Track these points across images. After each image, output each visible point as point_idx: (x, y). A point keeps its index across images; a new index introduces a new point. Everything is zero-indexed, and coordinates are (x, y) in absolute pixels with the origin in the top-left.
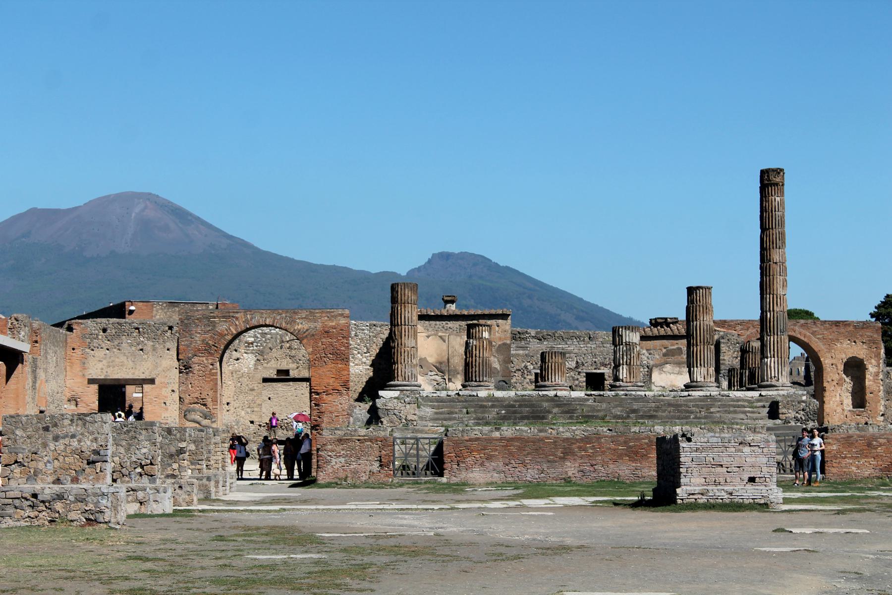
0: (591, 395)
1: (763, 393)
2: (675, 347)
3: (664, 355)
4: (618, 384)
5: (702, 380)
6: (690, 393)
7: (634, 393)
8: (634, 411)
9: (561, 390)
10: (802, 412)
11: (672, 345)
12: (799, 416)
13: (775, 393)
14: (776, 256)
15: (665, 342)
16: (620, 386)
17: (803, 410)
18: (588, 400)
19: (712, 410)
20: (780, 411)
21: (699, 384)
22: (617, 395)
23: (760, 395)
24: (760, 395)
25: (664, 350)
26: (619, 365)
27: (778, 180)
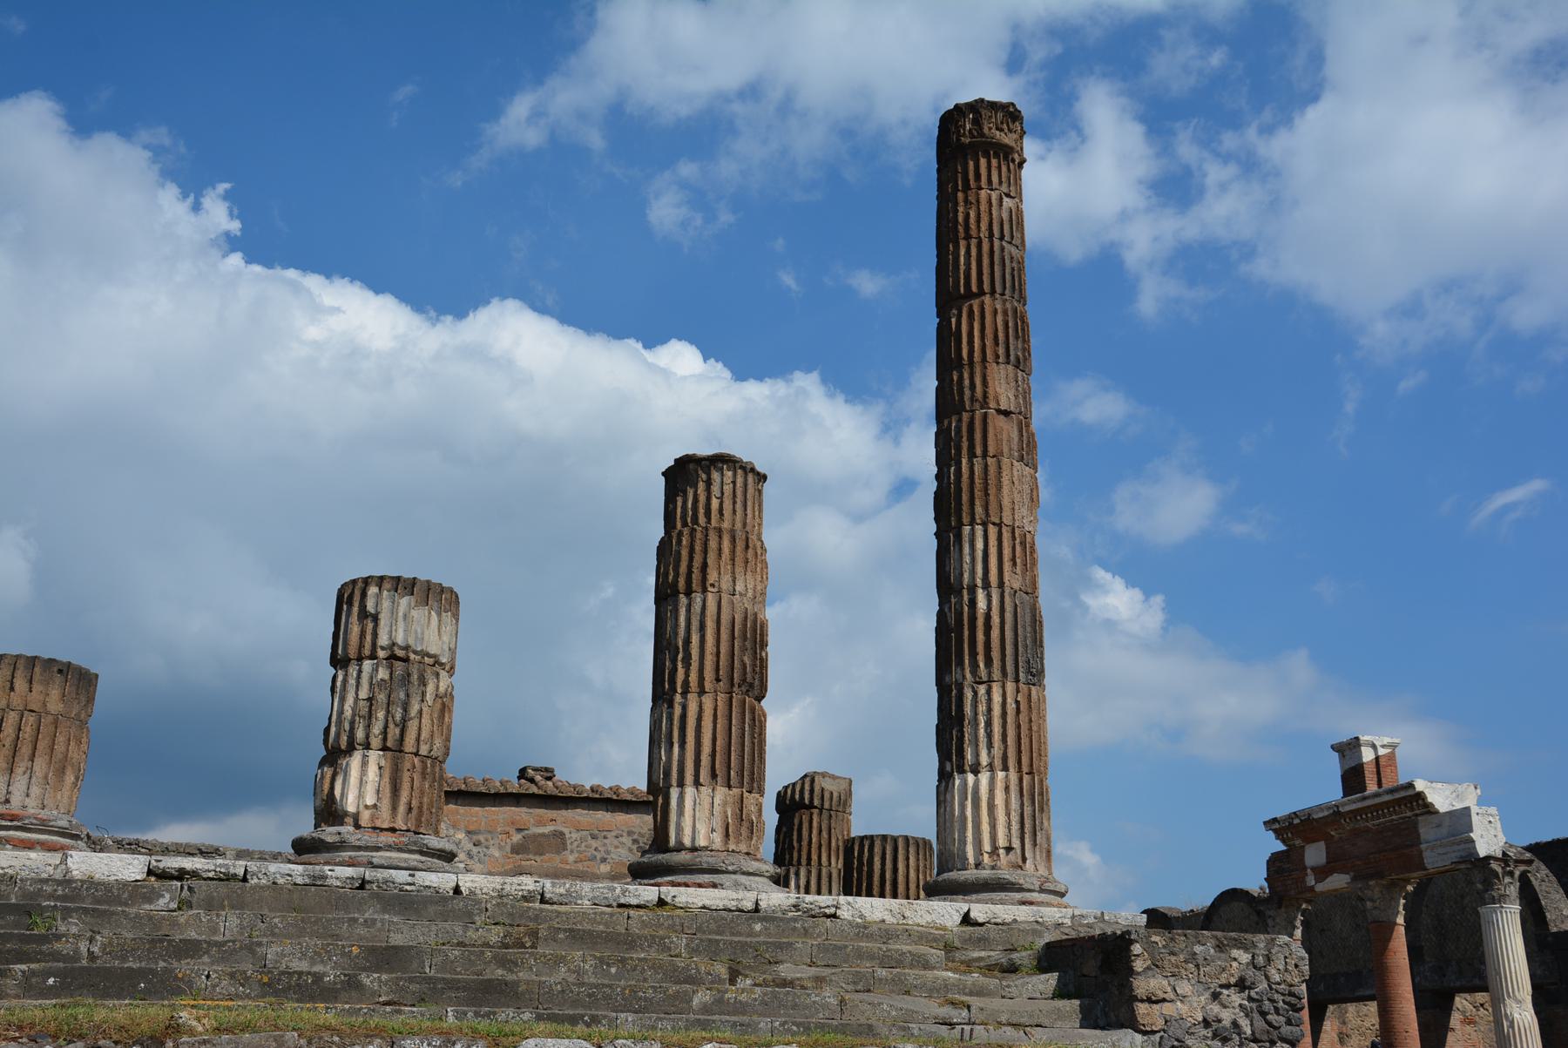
0: (181, 875)
1: (979, 912)
2: (547, 830)
3: (517, 850)
4: (329, 833)
5: (718, 838)
6: (668, 892)
7: (401, 876)
8: (385, 957)
9: (29, 846)
10: (1236, 998)
11: (540, 823)
12: (1227, 1016)
13: (1023, 914)
14: (1002, 388)
15: (522, 813)
16: (341, 846)
17: (1242, 985)
18: (152, 896)
19: (786, 970)
20: (1141, 986)
21: (705, 859)
22: (317, 881)
23: (966, 920)
24: (966, 920)
25: (517, 838)
26: (351, 748)
27: (1008, 139)
